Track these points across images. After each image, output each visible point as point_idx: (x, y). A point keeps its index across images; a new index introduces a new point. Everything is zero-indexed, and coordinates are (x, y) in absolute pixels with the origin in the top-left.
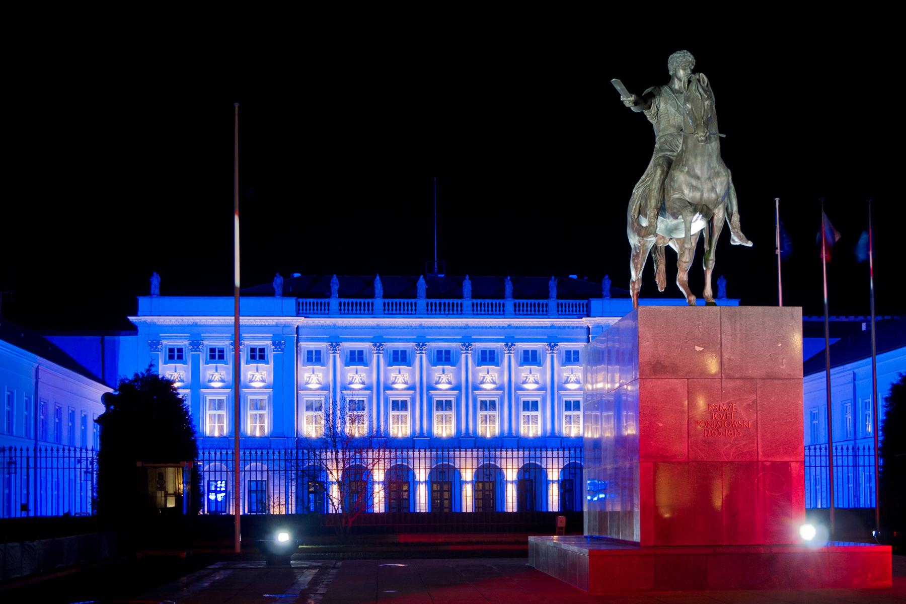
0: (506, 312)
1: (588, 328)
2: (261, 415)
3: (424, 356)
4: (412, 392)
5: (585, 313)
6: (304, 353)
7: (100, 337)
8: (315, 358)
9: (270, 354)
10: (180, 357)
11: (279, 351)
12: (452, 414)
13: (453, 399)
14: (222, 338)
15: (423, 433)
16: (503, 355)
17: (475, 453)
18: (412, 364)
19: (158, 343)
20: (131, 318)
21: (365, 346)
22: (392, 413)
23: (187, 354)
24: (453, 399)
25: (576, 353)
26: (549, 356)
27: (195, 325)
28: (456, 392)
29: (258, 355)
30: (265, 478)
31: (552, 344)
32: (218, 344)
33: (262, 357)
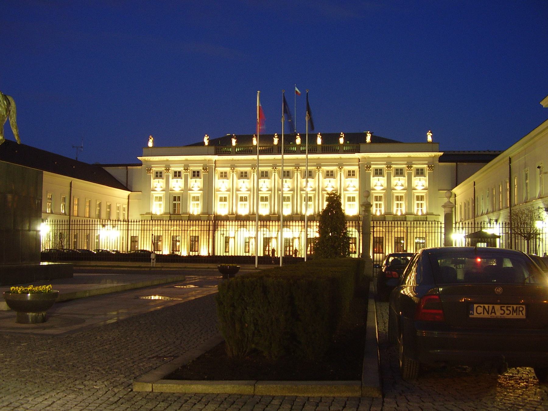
0: (318, 151)
1: (359, 159)
2: (198, 204)
3: (276, 174)
4: (270, 192)
5: (358, 151)
6: (219, 174)
7: (126, 167)
8: (224, 175)
9: (202, 174)
10: (161, 176)
11: (205, 172)
12: (290, 203)
13: (290, 195)
14: (180, 167)
15: (254, 213)
16: (315, 173)
17: (237, 223)
18: (271, 178)
19: (151, 170)
20: (139, 158)
21: (248, 169)
22: (260, 203)
23: (164, 175)
24: (290, 195)
25: (354, 172)
26: (339, 173)
27: (167, 161)
28: (292, 192)
29: (196, 174)
30: (161, 235)
31: (341, 167)
32: (178, 169)
33: (198, 176)
